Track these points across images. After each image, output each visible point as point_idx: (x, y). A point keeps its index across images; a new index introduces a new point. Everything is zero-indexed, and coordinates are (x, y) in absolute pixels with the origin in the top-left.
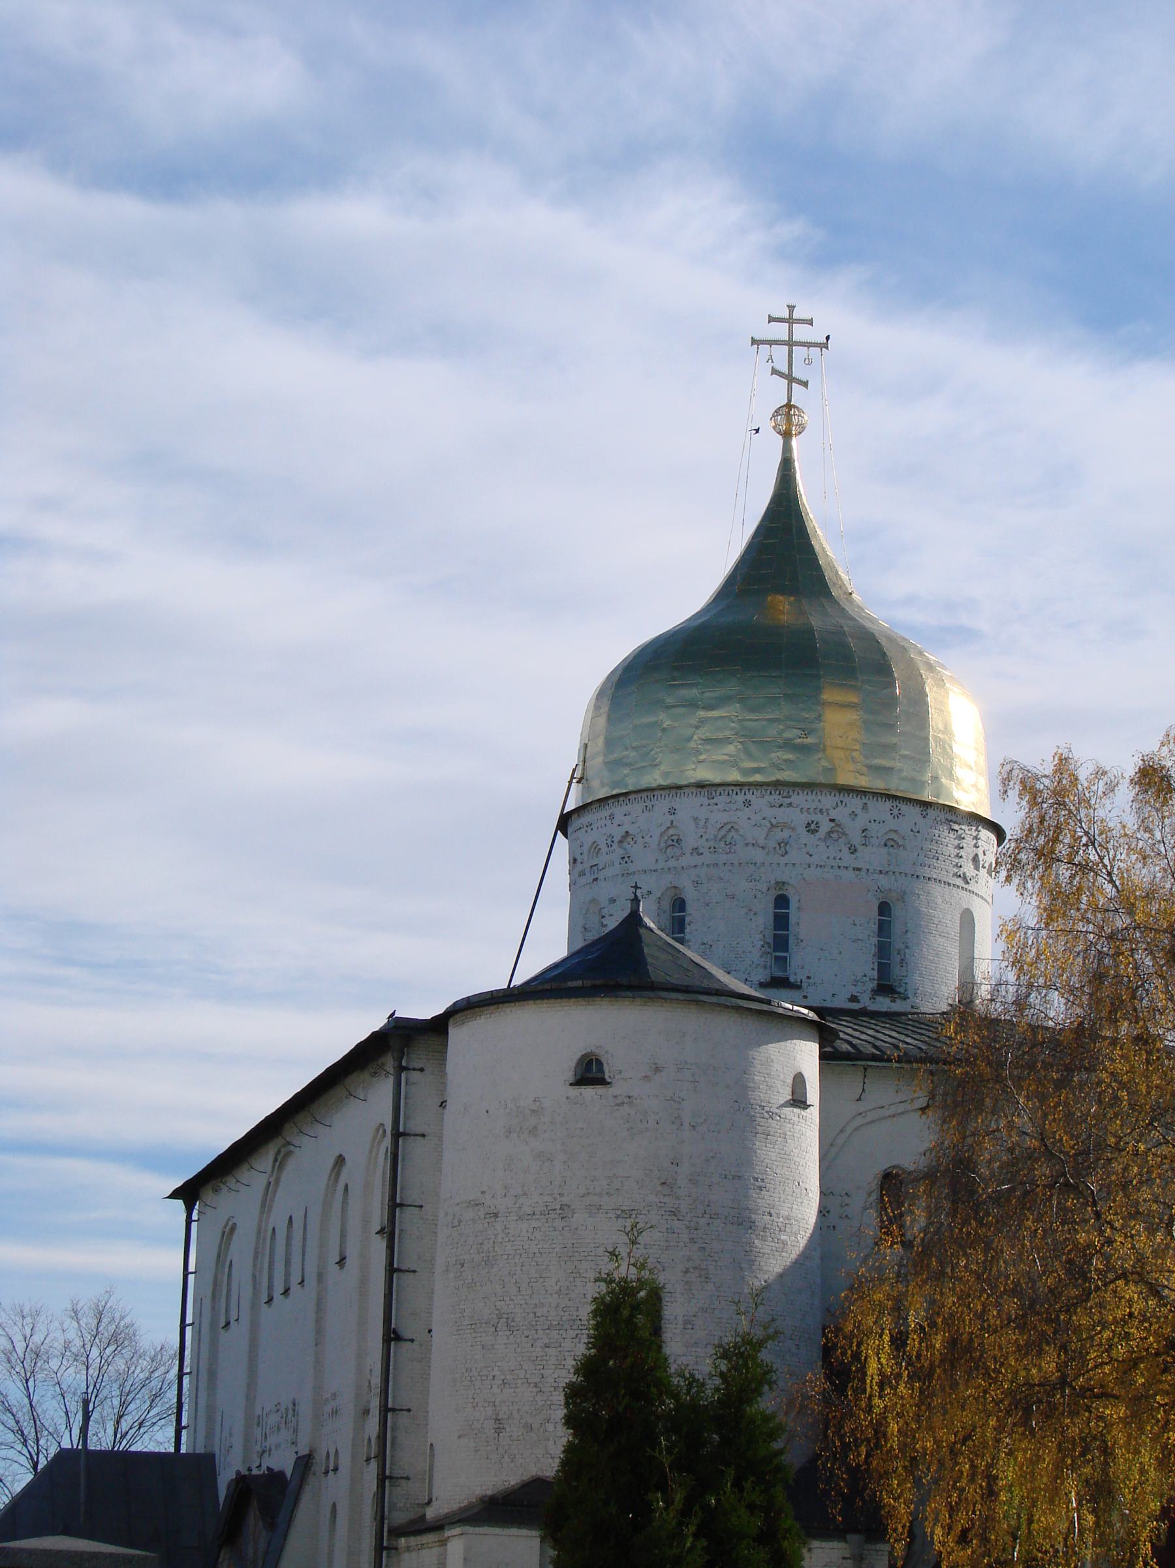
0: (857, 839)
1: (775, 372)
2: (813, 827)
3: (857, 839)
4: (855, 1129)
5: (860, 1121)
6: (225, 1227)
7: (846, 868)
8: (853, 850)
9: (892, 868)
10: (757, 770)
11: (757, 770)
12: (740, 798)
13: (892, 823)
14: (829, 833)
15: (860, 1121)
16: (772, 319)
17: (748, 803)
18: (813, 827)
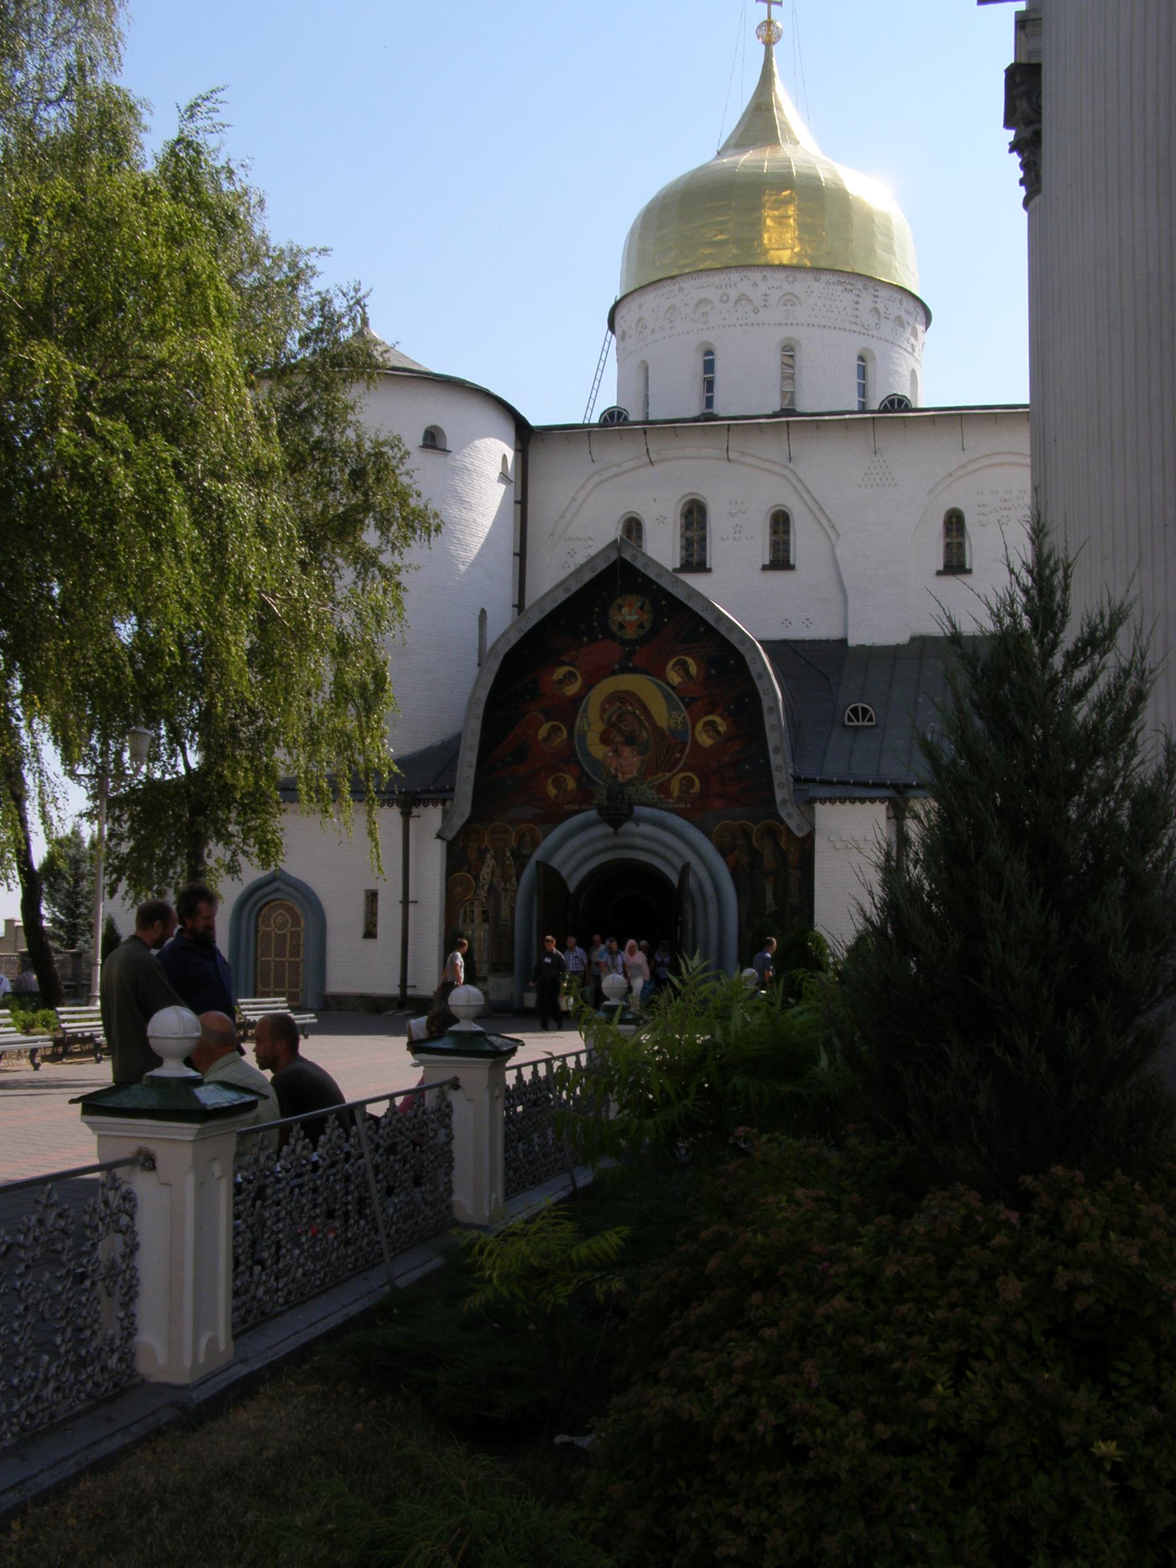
0: (758, 301)
2: (725, 298)
3: (758, 301)
4: (597, 484)
5: (597, 478)
7: (752, 325)
8: (756, 311)
9: (789, 321)
10: (689, 265)
11: (689, 265)
12: (676, 287)
13: (788, 288)
14: (738, 301)
15: (597, 478)
17: (681, 289)
18: (725, 298)
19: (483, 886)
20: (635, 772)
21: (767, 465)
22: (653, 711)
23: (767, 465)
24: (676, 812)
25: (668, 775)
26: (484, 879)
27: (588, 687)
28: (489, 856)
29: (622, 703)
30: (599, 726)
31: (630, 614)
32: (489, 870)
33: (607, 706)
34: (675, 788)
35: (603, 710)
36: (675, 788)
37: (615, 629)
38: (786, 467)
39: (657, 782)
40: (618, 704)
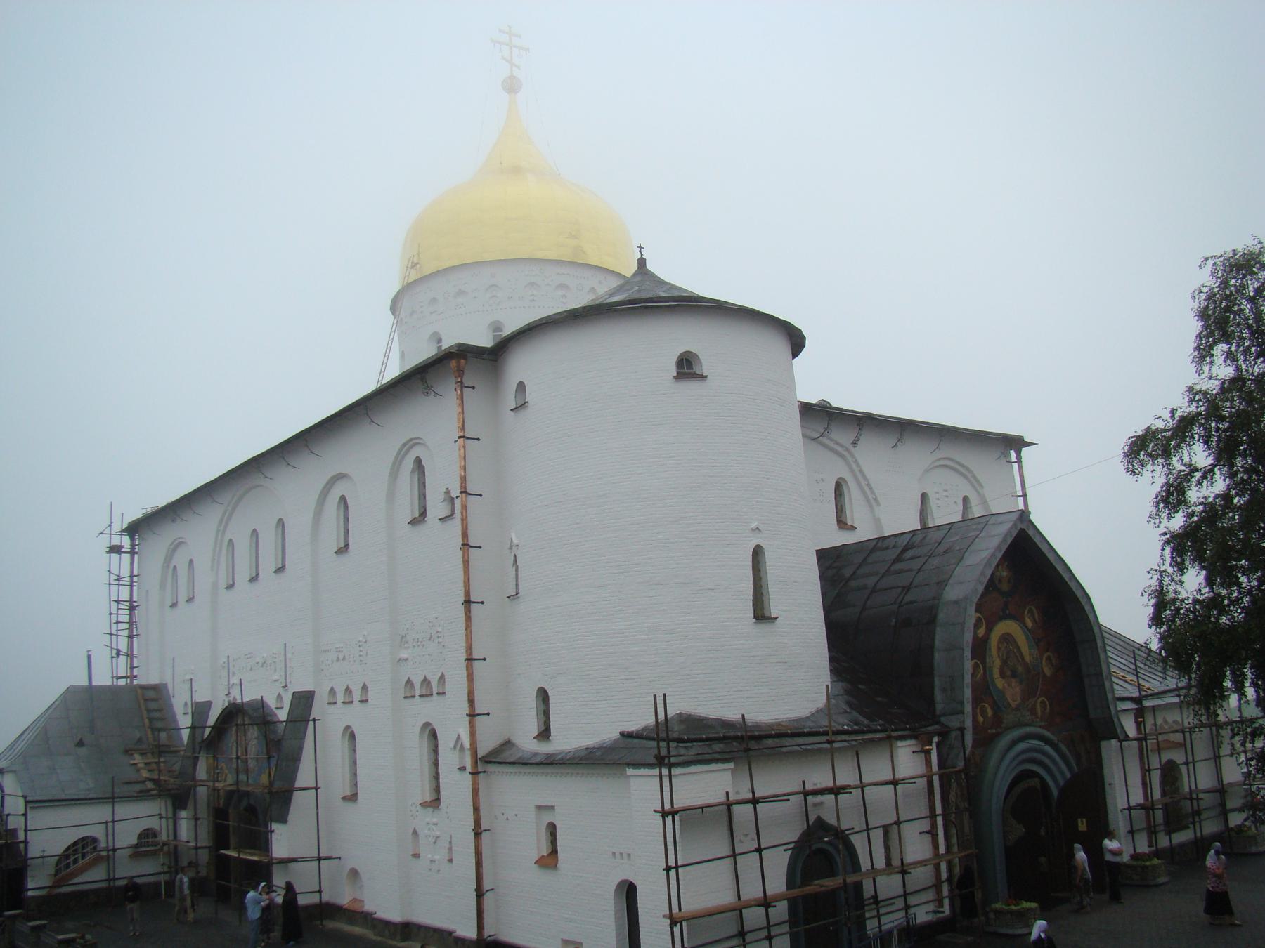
1: (504, 58)
6: (171, 545)
16: (501, 31)
19: (952, 807)
20: (1019, 699)
21: (839, 449)
22: (1023, 650)
23: (839, 449)
24: (1040, 727)
25: (1034, 699)
26: (952, 801)
27: (989, 630)
28: (953, 781)
29: (1008, 644)
30: (998, 663)
31: (1003, 571)
32: (954, 793)
33: (1000, 646)
34: (1039, 710)
35: (999, 649)
36: (1039, 710)
37: (997, 582)
38: (847, 450)
39: (1030, 706)
40: (1006, 644)
